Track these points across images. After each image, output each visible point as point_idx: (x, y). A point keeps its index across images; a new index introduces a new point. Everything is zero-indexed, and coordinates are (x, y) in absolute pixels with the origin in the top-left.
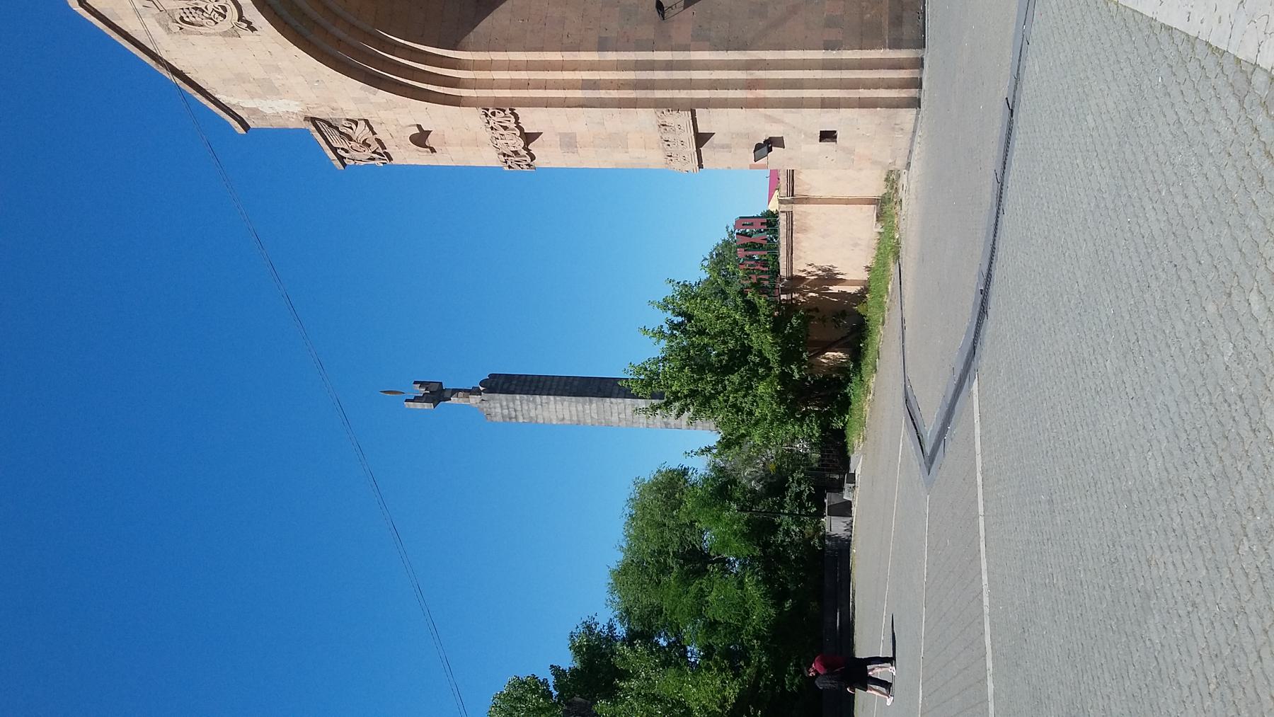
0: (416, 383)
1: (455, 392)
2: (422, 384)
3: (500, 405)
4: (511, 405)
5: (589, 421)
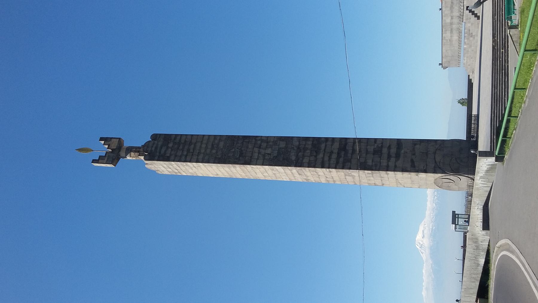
0: (101, 139)
1: (130, 150)
2: (106, 140)
3: (162, 167)
4: (170, 166)
5: (239, 176)
